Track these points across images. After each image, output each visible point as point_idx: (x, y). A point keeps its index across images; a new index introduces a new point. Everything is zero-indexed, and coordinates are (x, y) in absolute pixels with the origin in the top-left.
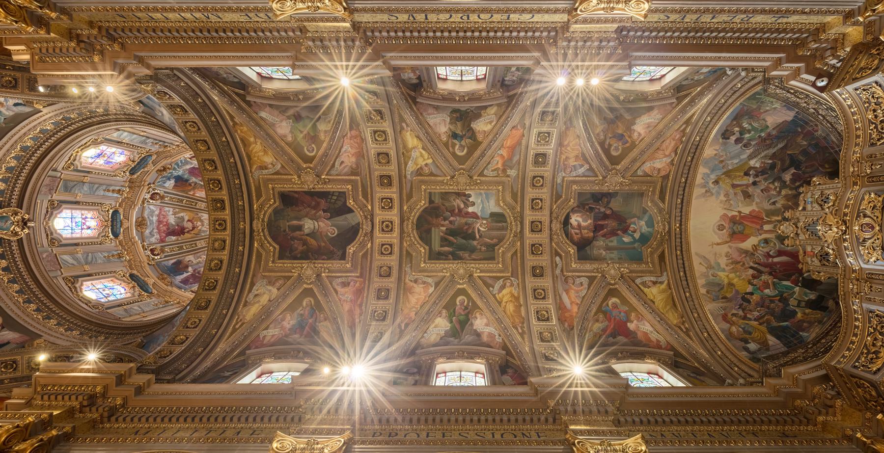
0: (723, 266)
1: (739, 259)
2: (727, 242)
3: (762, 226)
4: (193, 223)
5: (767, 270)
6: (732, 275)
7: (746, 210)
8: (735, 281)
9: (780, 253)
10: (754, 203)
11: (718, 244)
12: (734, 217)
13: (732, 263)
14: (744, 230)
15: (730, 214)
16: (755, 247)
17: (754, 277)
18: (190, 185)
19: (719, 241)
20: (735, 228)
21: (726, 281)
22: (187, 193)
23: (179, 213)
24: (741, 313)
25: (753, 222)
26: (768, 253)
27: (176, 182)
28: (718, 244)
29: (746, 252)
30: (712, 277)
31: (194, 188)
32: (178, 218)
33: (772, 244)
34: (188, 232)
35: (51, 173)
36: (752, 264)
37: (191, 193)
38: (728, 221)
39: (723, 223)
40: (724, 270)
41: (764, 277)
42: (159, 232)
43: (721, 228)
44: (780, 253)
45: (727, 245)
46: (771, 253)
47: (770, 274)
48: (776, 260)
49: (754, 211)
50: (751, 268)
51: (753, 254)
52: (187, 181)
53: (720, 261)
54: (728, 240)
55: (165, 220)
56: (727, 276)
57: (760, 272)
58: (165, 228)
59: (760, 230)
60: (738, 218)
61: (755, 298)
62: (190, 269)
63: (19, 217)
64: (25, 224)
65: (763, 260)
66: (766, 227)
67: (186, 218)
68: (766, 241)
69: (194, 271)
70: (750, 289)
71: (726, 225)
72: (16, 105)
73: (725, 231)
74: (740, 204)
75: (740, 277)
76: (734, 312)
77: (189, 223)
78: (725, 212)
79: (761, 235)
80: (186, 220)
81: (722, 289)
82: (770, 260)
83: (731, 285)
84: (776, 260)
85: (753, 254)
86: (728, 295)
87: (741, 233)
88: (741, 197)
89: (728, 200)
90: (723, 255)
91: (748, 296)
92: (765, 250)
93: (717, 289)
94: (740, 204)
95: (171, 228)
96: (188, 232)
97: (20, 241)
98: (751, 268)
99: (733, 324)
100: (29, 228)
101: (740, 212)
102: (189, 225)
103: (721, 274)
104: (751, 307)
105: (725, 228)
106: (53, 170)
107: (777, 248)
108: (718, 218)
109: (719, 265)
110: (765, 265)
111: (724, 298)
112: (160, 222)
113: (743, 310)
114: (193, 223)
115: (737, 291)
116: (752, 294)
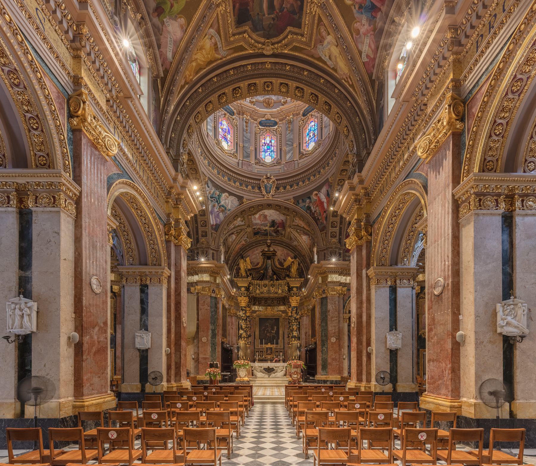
35: (240, 167)
63: (265, 180)
64: (268, 178)
72: (209, 187)
97: (277, 180)
100: (270, 176)
106: (238, 166)
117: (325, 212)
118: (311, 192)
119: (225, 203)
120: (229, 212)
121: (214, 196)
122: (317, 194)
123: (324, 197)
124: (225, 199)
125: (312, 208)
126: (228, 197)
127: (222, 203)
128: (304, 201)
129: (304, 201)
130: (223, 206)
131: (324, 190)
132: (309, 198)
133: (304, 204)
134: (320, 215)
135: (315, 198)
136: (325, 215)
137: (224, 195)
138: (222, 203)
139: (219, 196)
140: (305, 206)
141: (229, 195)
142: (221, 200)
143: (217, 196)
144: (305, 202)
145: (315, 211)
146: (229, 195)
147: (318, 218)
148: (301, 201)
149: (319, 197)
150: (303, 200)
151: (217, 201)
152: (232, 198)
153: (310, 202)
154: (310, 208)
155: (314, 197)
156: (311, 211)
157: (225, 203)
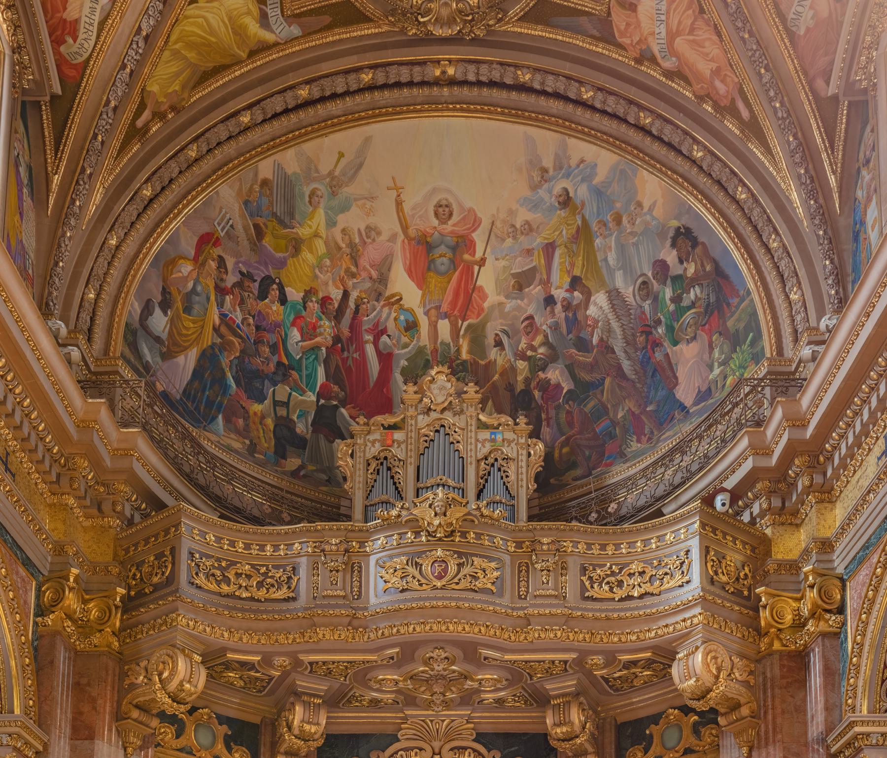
0: (342, 220)
1: (364, 262)
2: (405, 228)
3: (446, 316)
5: (346, 332)
6: (320, 246)
7: (486, 279)
8: (307, 256)
9: (386, 359)
10: (502, 299)
11: (399, 204)
12: (471, 246)
13: (352, 245)
14: (438, 273)
15: (479, 238)
16: (396, 301)
17: (325, 301)
19: (407, 207)
20: (442, 249)
21: (303, 232)
24: (231, 279)
25: (456, 294)
26: (384, 331)
28: (399, 204)
29: (383, 279)
30: (307, 191)
33: (405, 340)
36: (354, 295)
38: (460, 230)
39: (455, 218)
40: (331, 223)
41: (327, 326)
43: (443, 211)
44: (386, 359)
45: (398, 229)
46: (384, 338)
47: (337, 339)
48: (370, 349)
49: (484, 297)
50: (346, 295)
51: (379, 296)
53: (354, 210)
54: (412, 232)
56: (316, 235)
57: (338, 316)
59: (436, 313)
60: (467, 257)
61: (274, 310)
65: (367, 321)
66: (444, 326)
68: (411, 327)
70: (294, 294)
71: (448, 227)
73: (435, 222)
74: (502, 263)
75: (320, 267)
76: (230, 263)
78: (485, 225)
79: (427, 313)
81: (281, 222)
82: (369, 337)
83: (296, 246)
84: (370, 349)
85: (379, 296)
86: (267, 241)
87: (430, 265)
88: (520, 265)
89: (514, 232)
90: (371, 220)
91: (274, 292)
92: (391, 325)
93: (279, 209)
94: (502, 263)
98: (346, 295)
99: (198, 260)
101: (482, 262)
103: (320, 217)
104: (251, 302)
105: (443, 222)
107: (397, 352)
108: (468, 204)
109: (345, 208)
110: (354, 326)
111: (259, 232)
113: (239, 285)
115: (282, 264)
116: (283, 300)
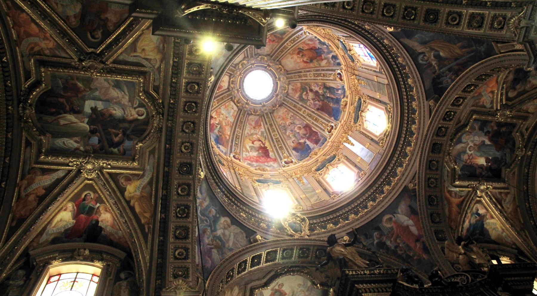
4: (255, 141)
18: (221, 135)
22: (229, 140)
23: (246, 149)
27: (220, 144)
31: (223, 134)
32: (251, 150)
34: (264, 144)
37: (228, 138)
42: (268, 162)
52: (217, 136)
55: (255, 158)
58: (263, 159)
62: (302, 141)
67: (251, 145)
69: (303, 138)
77: (255, 143)
80: (252, 145)
95: (262, 154)
96: (264, 144)
102: (257, 144)
112: (257, 161)
114: (255, 141)
117: (417, 240)
118: (379, 218)
119: (224, 234)
120: (230, 254)
121: (207, 213)
122: (390, 219)
123: (406, 218)
124: (225, 228)
125: (388, 243)
126: (230, 227)
127: (219, 232)
128: (368, 236)
129: (368, 236)
130: (219, 238)
131: (403, 207)
132: (378, 229)
133: (369, 241)
134: (410, 249)
135: (389, 226)
136: (418, 245)
137: (224, 220)
138: (219, 232)
139: (216, 220)
140: (373, 244)
141: (233, 223)
142: (218, 227)
143: (211, 216)
144: (371, 237)
145: (396, 247)
146: (233, 223)
147: (408, 256)
148: (362, 238)
149: (396, 222)
150: (366, 235)
151: (210, 226)
152: (235, 229)
153: (381, 235)
154: (384, 243)
155: (386, 225)
156: (388, 249)
157: (224, 234)
